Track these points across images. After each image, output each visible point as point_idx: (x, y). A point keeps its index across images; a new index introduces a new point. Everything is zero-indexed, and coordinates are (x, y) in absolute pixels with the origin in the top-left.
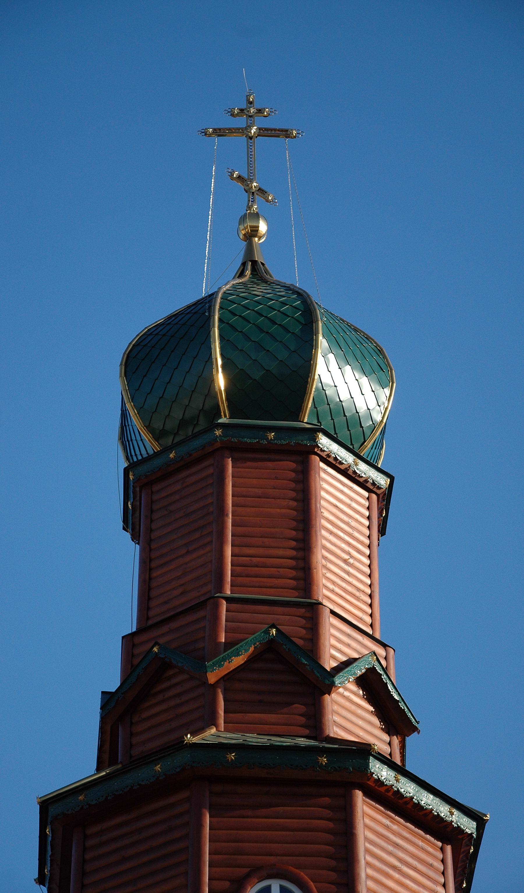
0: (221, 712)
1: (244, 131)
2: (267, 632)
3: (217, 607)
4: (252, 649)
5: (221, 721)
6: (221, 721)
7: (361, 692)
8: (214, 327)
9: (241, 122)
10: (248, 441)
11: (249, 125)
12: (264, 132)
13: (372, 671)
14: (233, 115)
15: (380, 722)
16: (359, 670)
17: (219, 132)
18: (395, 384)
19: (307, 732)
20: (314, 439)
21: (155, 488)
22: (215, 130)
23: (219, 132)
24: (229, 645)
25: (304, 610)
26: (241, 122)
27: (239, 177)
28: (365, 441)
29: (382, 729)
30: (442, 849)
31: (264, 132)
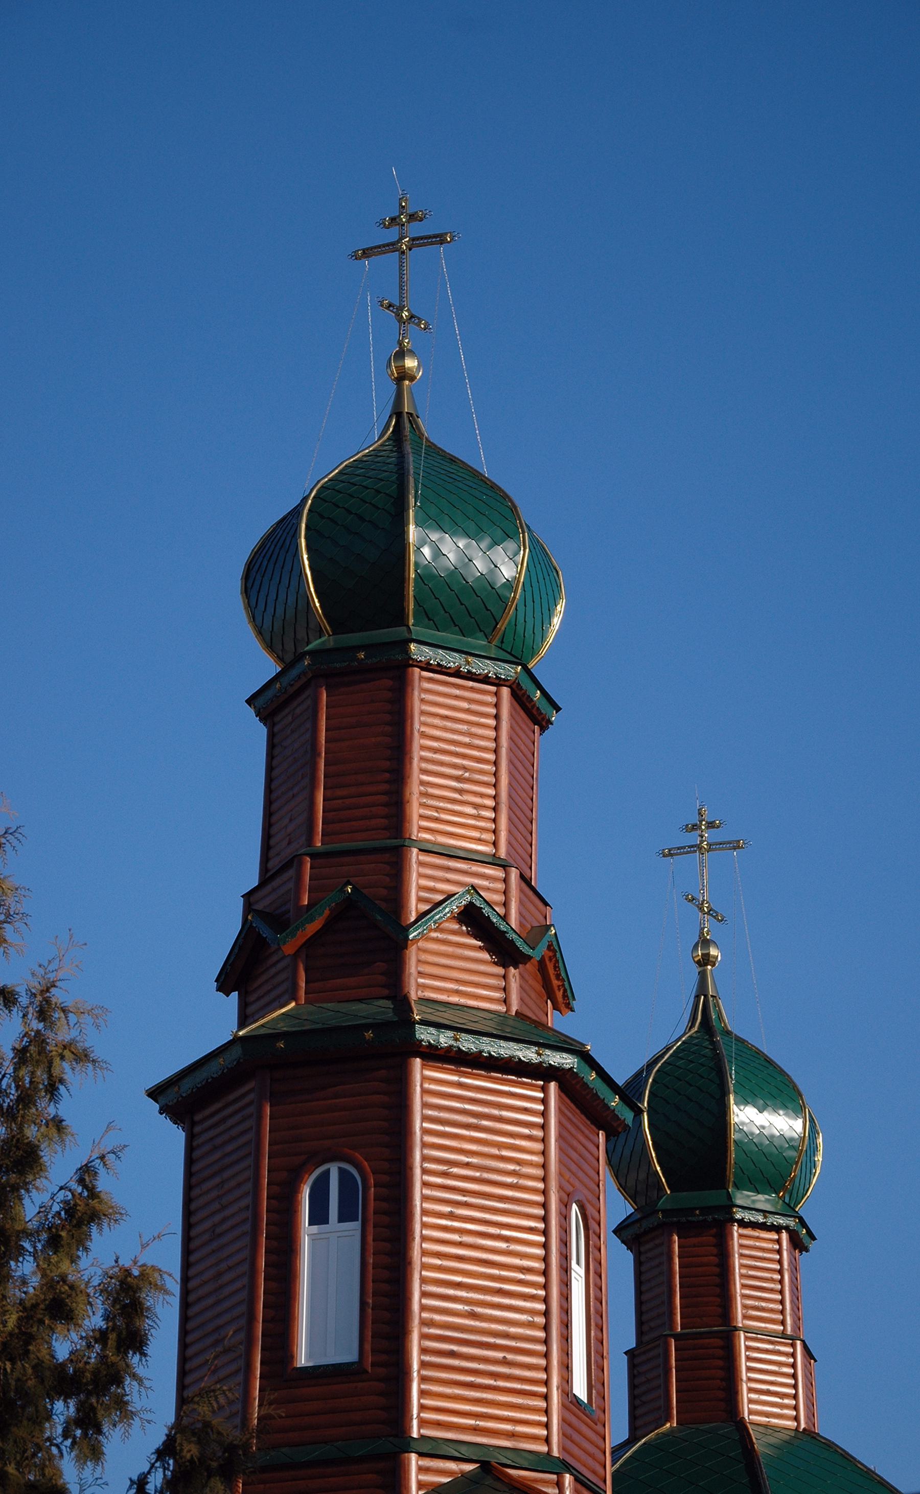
0: (303, 985)
1: (392, 247)
2: (342, 890)
3: (301, 864)
4: (327, 912)
5: (302, 993)
6: (302, 993)
7: (464, 928)
8: (300, 537)
9: (392, 235)
10: (338, 665)
11: (406, 235)
12: (416, 242)
13: (470, 906)
14: (385, 227)
15: (491, 956)
16: (454, 907)
17: (367, 253)
18: (527, 550)
19: (386, 992)
20: (407, 651)
21: (277, 719)
22: (364, 250)
23: (367, 253)
24: (310, 906)
25: (388, 855)
26: (392, 235)
27: (390, 305)
28: (497, 624)
29: (495, 963)
30: (544, 1089)
31: (416, 242)
